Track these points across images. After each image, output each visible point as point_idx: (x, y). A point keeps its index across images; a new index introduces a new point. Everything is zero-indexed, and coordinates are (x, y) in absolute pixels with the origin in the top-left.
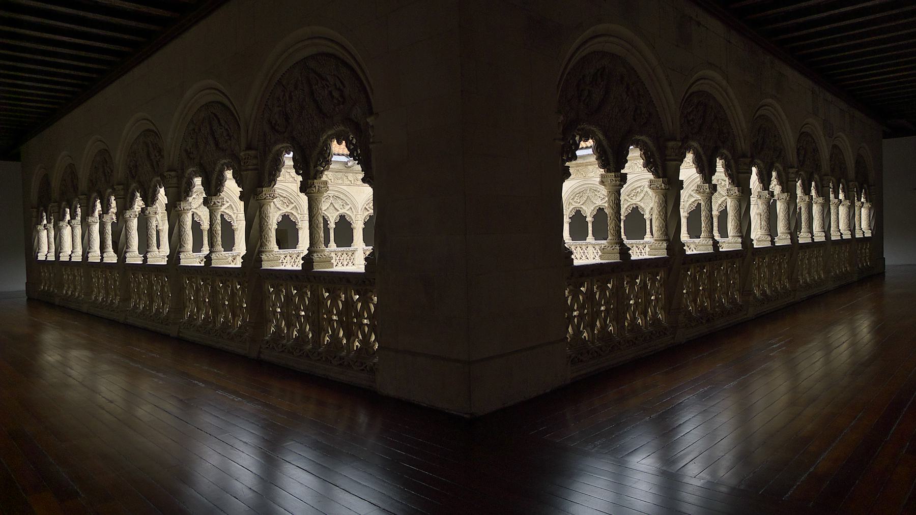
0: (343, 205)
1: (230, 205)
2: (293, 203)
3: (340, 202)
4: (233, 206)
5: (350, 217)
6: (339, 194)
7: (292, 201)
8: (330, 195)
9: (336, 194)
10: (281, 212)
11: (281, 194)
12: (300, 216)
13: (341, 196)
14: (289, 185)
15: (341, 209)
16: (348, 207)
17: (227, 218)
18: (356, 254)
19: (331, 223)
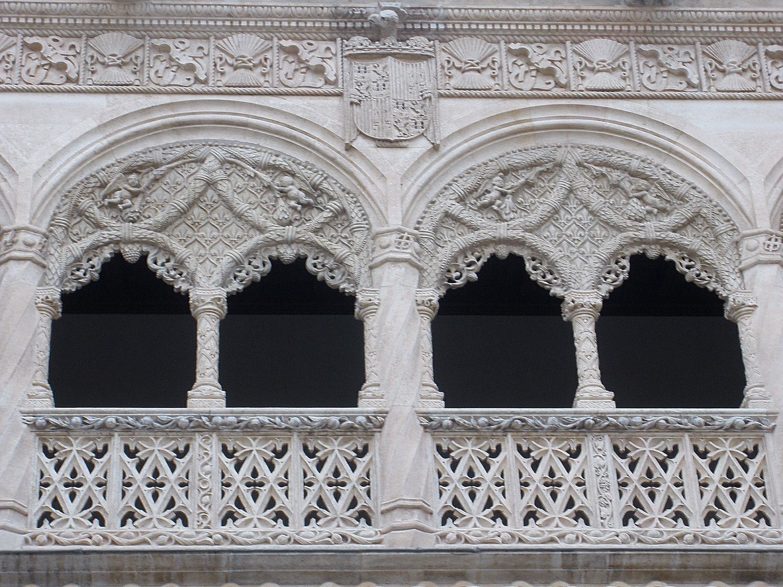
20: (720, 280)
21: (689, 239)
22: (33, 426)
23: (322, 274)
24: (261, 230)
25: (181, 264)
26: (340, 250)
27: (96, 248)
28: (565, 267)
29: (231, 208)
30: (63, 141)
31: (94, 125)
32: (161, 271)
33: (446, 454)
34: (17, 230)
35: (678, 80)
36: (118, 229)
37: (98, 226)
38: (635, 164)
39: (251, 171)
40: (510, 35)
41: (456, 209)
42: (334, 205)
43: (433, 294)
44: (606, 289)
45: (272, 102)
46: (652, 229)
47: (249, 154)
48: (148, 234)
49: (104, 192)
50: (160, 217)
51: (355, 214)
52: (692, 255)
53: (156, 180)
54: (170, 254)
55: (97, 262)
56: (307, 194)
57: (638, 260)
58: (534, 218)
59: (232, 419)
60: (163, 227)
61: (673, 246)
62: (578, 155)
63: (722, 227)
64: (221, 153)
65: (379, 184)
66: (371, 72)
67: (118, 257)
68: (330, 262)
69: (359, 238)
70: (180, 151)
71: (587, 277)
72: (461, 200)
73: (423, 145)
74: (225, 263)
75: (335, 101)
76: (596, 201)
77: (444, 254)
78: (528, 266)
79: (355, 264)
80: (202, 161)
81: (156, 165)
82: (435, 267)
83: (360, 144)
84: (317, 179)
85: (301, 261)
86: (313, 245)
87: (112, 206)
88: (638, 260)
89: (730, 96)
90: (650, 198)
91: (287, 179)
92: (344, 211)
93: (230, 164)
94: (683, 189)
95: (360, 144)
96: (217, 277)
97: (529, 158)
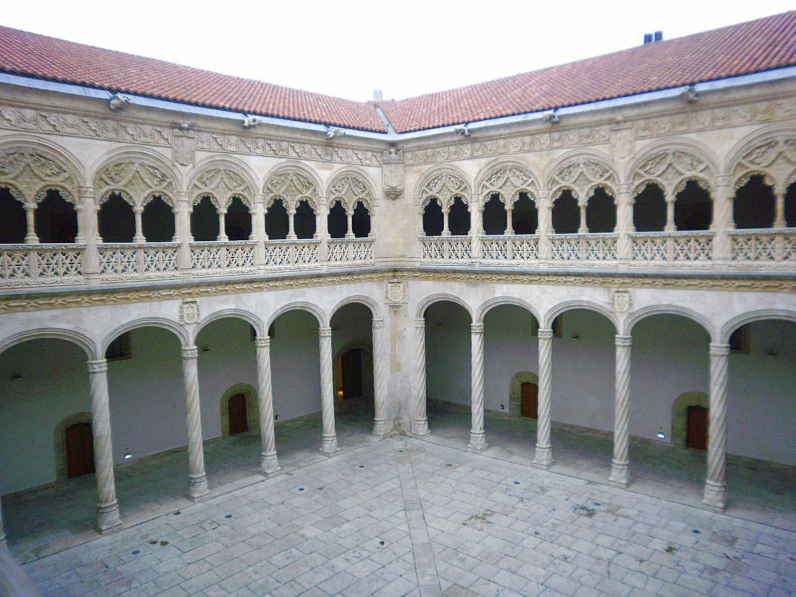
0: (691, 164)
1: (533, 181)
2: (607, 171)
3: (688, 160)
4: (536, 183)
5: (706, 182)
6: (685, 147)
7: (607, 168)
8: (668, 152)
9: (680, 148)
10: (593, 184)
11: (592, 161)
12: (618, 187)
13: (690, 150)
14: (600, 147)
15: (689, 170)
16: (702, 167)
17: (530, 196)
18: (716, 241)
19: (668, 194)
20: (250, 205)
21: (246, 194)
22: (99, 248)
23: (165, 201)
24: (151, 188)
25: (131, 198)
26: (171, 195)
27: (107, 192)
28: (220, 200)
29: (142, 180)
30: (97, 157)
31: (105, 152)
32: (125, 199)
33: (193, 252)
34: (87, 187)
35: (248, 149)
36: (113, 186)
37: (107, 184)
38: (236, 172)
39: (147, 167)
40: (213, 133)
41: (197, 183)
42: (168, 180)
43: (192, 210)
44: (227, 206)
45: (154, 148)
46: (239, 190)
47: (146, 162)
48: (122, 188)
49: (108, 172)
50: (124, 182)
51: (173, 183)
52: (245, 198)
53: (122, 169)
54: (128, 194)
55: (108, 195)
56: (163, 177)
57: (234, 198)
58: (213, 186)
59: (147, 246)
60: (124, 186)
61: (241, 195)
62: (224, 168)
63: (252, 190)
64: (139, 161)
65: (181, 177)
66: (179, 141)
67: (113, 193)
68: (167, 198)
69: (175, 191)
70: (128, 160)
71: (223, 204)
72: (198, 180)
73: (192, 165)
74: (143, 197)
75: (170, 149)
76: (227, 183)
77: (194, 196)
78: (211, 200)
79: (174, 199)
80: (134, 163)
81: (121, 164)
82: (192, 201)
83: (177, 164)
84: (164, 172)
85: (160, 196)
86: (163, 192)
87: (111, 178)
88: (234, 198)
89: (258, 155)
90: (239, 182)
91: (157, 171)
92: (171, 182)
93: (142, 165)
94: (245, 179)
95: (177, 164)
96: (141, 203)
97: (213, 168)
